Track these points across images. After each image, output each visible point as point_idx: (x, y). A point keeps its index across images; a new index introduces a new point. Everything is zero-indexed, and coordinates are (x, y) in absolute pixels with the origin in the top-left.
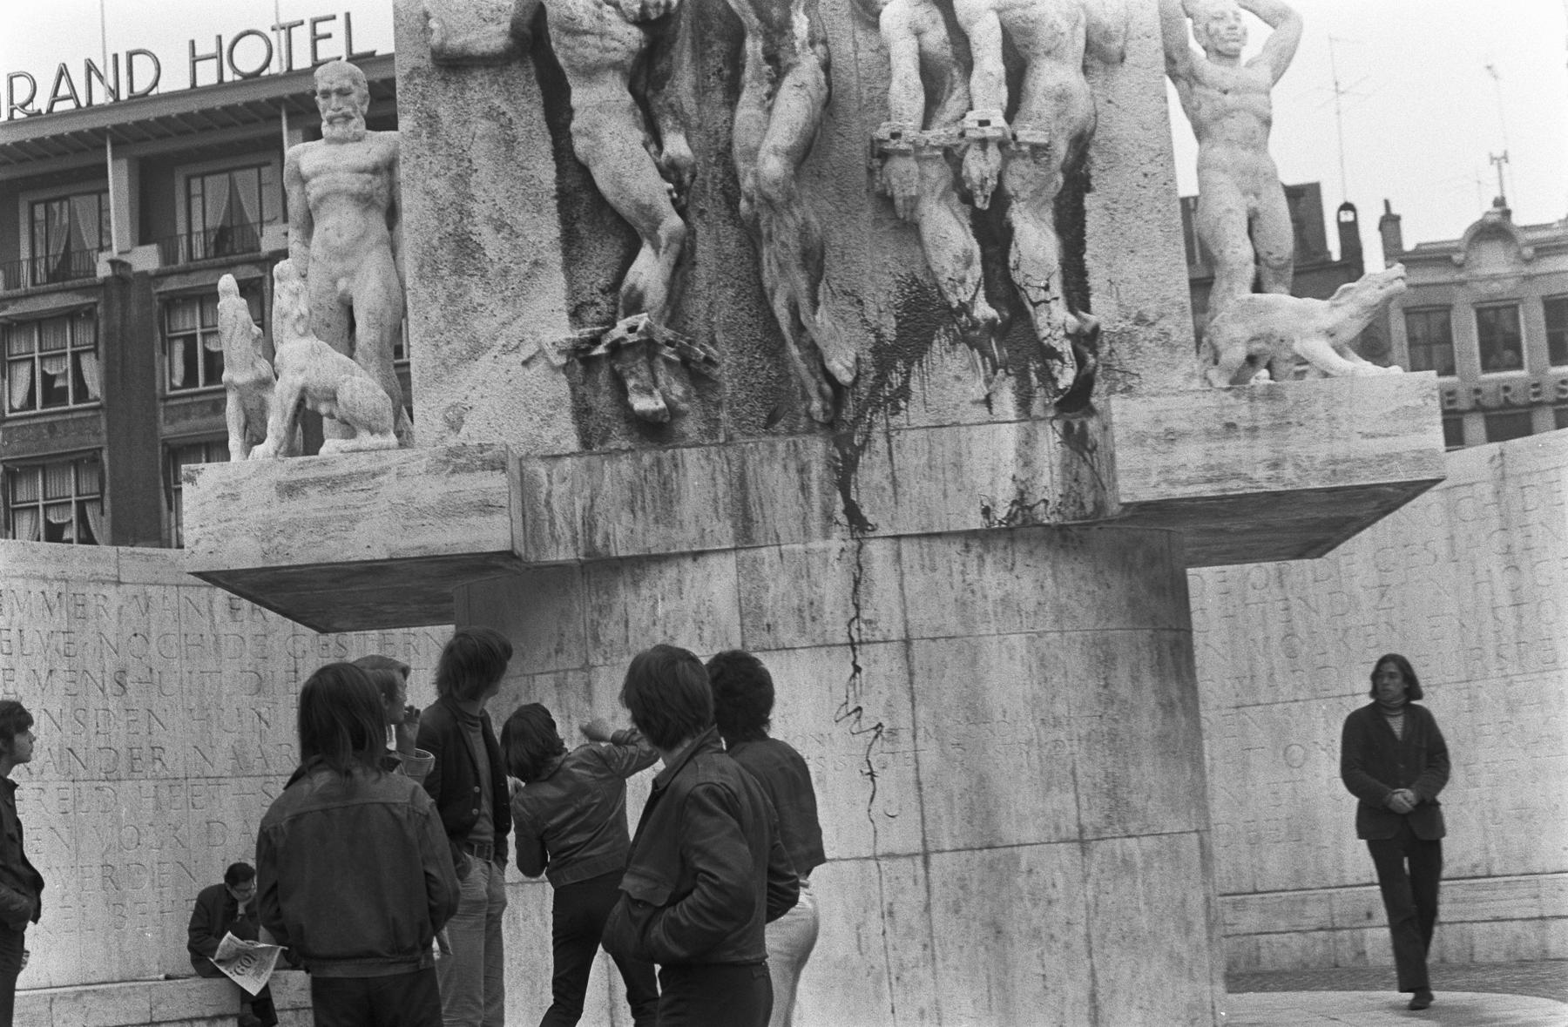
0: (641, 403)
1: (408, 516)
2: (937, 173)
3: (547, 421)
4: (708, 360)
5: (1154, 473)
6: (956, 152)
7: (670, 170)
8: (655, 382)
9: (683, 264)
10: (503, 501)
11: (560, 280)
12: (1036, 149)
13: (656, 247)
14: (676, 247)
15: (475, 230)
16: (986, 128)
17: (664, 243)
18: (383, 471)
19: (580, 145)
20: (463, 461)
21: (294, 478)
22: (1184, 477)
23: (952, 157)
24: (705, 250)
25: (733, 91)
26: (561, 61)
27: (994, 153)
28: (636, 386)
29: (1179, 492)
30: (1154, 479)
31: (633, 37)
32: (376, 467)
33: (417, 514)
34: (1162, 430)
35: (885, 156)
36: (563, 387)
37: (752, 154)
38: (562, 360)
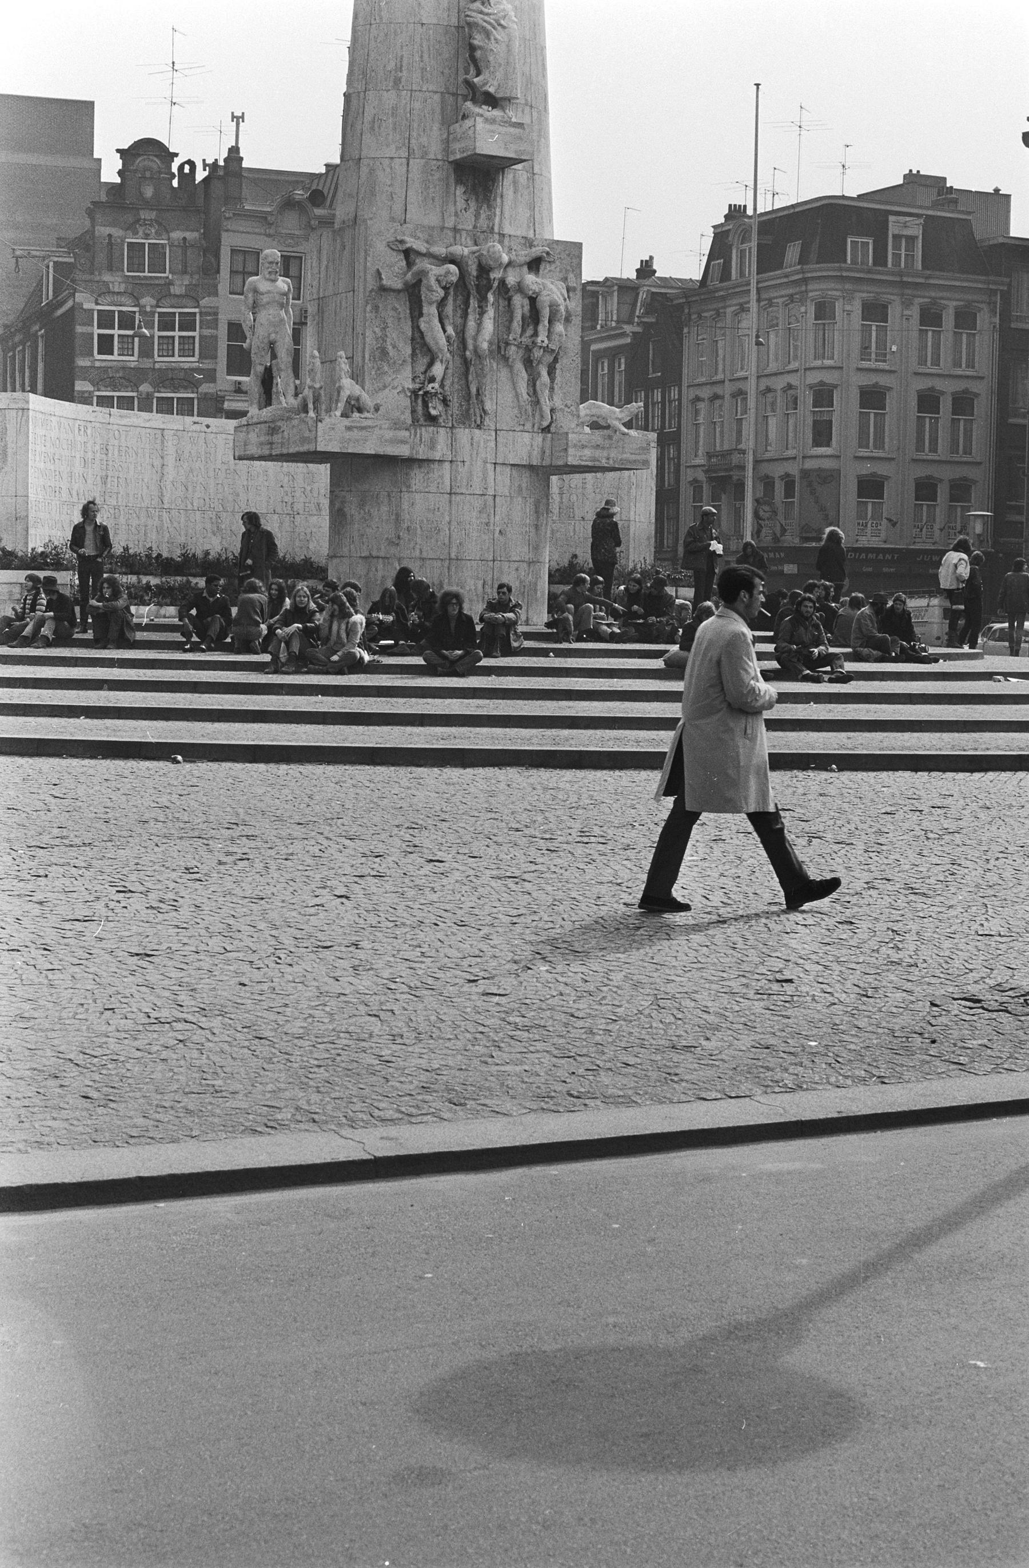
0: (433, 412)
2: (521, 353)
3: (403, 413)
7: (448, 339)
9: (446, 368)
11: (409, 368)
12: (553, 351)
13: (442, 361)
23: (528, 350)
24: (451, 365)
25: (465, 315)
29: (583, 463)
31: (442, 293)
35: (507, 344)
36: (407, 402)
37: (475, 339)
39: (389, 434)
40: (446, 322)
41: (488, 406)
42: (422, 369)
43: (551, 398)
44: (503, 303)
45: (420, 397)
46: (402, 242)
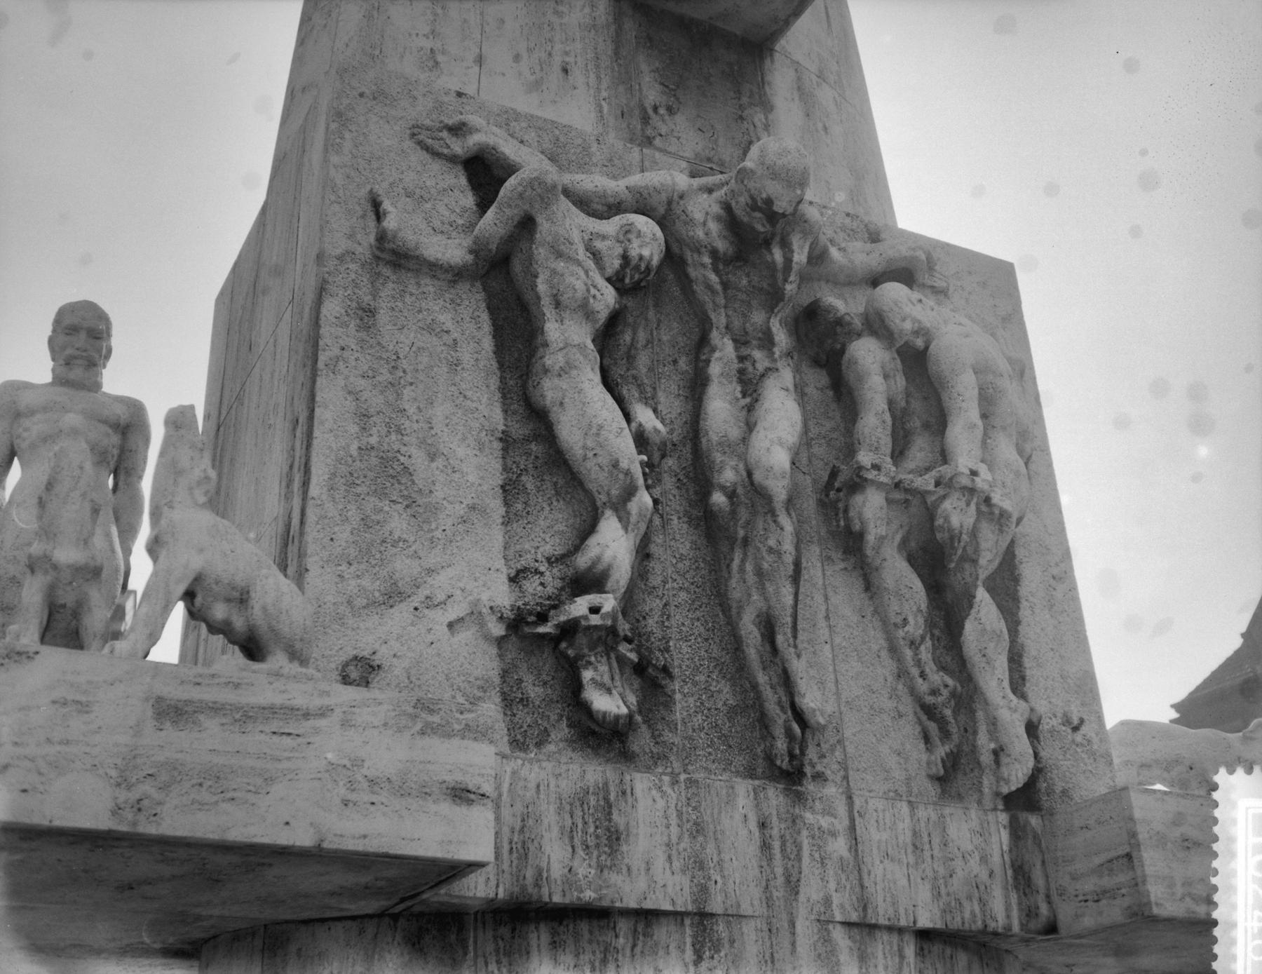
6: (930, 499)
7: (641, 440)
10: (487, 788)
15: (403, 449)
17: (633, 519)
18: (324, 712)
19: (549, 390)
20: (436, 719)
21: (185, 696)
25: (697, 387)
26: (542, 287)
30: (1179, 891)
32: (317, 702)
33: (365, 785)
34: (1178, 835)
38: (498, 630)
39: (388, 753)
41: (811, 699)
42: (553, 546)
43: (1018, 683)
44: (817, 380)
45: (544, 643)
46: (458, 130)
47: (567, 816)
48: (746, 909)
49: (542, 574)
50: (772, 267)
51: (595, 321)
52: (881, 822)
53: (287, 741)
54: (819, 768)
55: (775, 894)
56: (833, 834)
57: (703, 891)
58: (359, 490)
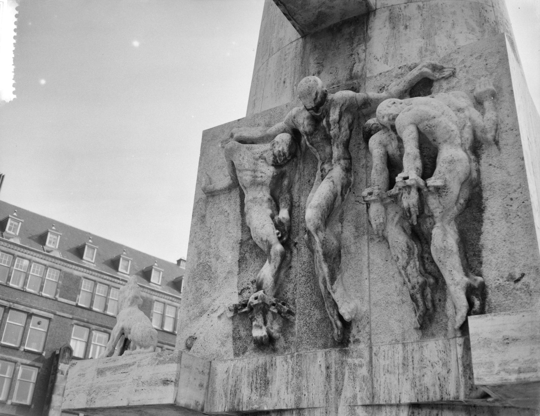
1: (138, 385)
4: (290, 312)
5: (497, 365)
7: (278, 225)
8: (265, 323)
11: (236, 279)
14: (279, 259)
16: (407, 181)
17: (273, 257)
20: (162, 359)
21: (104, 367)
22: (517, 368)
27: (414, 194)
28: (256, 325)
30: (496, 368)
40: (282, 205)
47: (251, 378)
48: (317, 404)
49: (249, 288)
50: (324, 128)
51: (266, 185)
52: (386, 356)
53: (124, 374)
54: (357, 337)
55: (330, 396)
56: (361, 366)
57: (299, 399)
58: (196, 279)
